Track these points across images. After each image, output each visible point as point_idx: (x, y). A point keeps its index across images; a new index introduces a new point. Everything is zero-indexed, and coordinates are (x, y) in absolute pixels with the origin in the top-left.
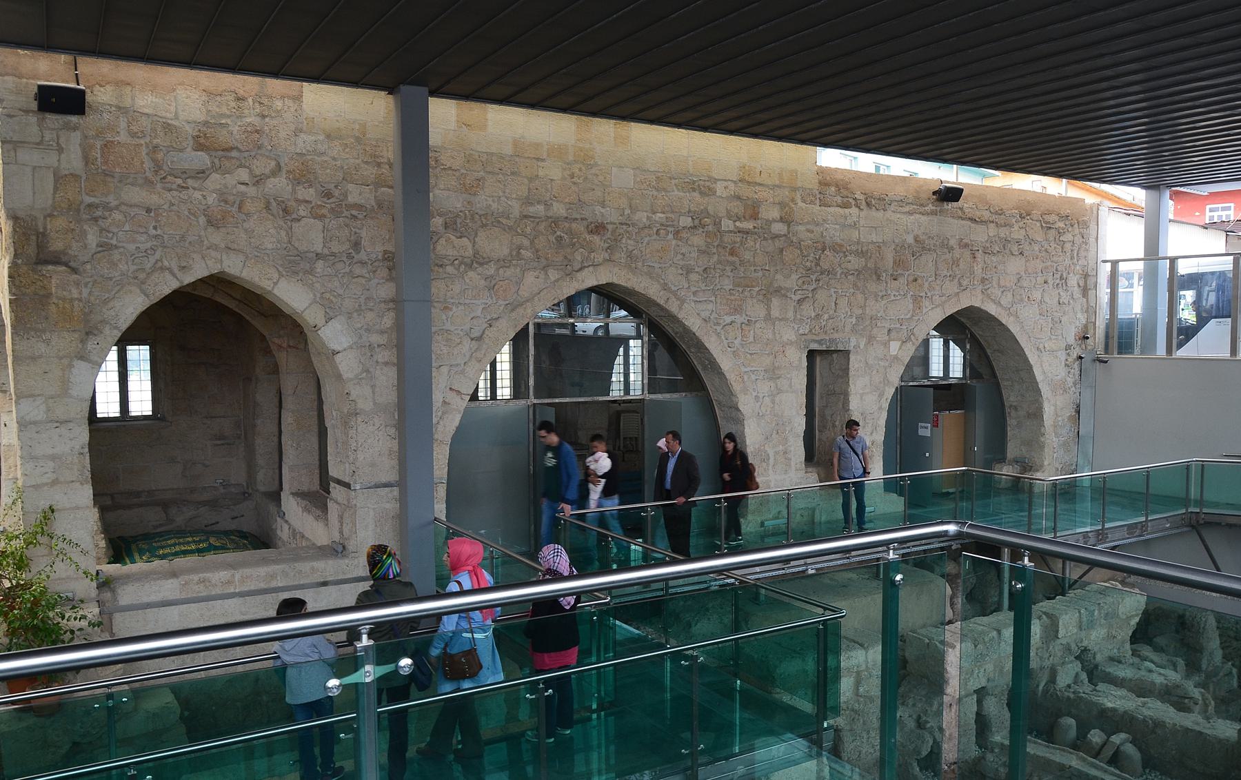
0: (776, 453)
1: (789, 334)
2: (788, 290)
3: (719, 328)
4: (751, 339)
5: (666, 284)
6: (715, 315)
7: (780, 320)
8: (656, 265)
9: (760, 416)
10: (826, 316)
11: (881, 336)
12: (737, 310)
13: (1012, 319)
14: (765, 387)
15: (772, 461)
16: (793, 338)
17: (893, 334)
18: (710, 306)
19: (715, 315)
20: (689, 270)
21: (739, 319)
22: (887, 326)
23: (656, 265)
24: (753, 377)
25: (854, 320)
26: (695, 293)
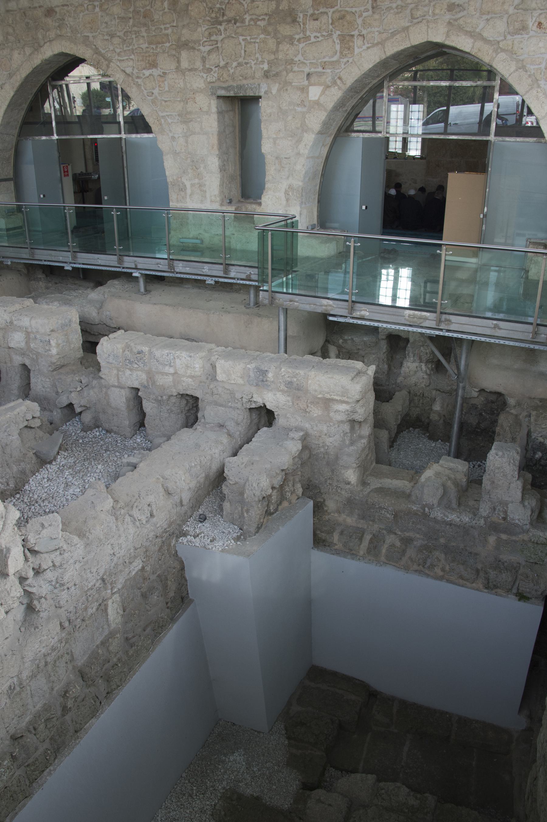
0: (192, 185)
1: (198, 82)
2: (197, 42)
3: (140, 81)
4: (167, 89)
5: (97, 49)
6: (136, 71)
7: (190, 70)
8: (90, 35)
9: (176, 154)
10: (235, 64)
11: (299, 80)
12: (153, 65)
13: (502, 56)
14: (178, 129)
15: (189, 191)
16: (202, 85)
17: (313, 79)
18: (131, 63)
19: (136, 71)
20: (112, 36)
21: (156, 72)
22: (307, 70)
23: (90, 35)
24: (170, 121)
25: (266, 67)
26: (119, 54)
